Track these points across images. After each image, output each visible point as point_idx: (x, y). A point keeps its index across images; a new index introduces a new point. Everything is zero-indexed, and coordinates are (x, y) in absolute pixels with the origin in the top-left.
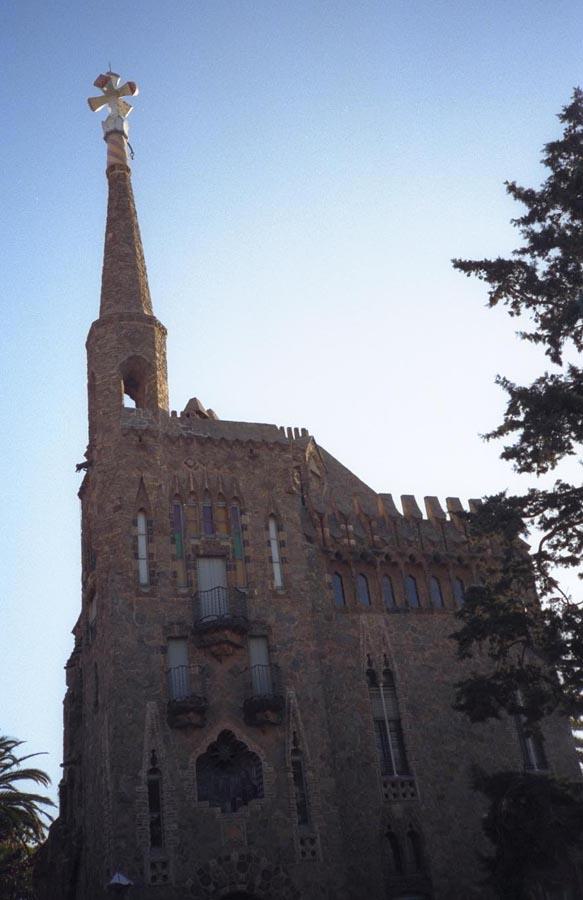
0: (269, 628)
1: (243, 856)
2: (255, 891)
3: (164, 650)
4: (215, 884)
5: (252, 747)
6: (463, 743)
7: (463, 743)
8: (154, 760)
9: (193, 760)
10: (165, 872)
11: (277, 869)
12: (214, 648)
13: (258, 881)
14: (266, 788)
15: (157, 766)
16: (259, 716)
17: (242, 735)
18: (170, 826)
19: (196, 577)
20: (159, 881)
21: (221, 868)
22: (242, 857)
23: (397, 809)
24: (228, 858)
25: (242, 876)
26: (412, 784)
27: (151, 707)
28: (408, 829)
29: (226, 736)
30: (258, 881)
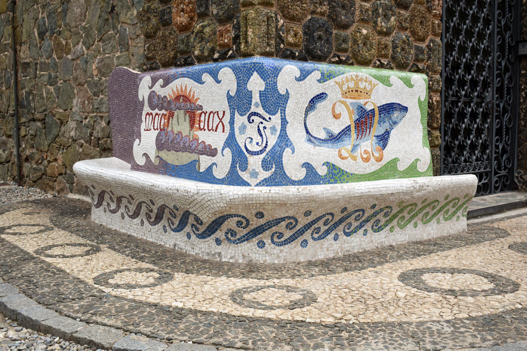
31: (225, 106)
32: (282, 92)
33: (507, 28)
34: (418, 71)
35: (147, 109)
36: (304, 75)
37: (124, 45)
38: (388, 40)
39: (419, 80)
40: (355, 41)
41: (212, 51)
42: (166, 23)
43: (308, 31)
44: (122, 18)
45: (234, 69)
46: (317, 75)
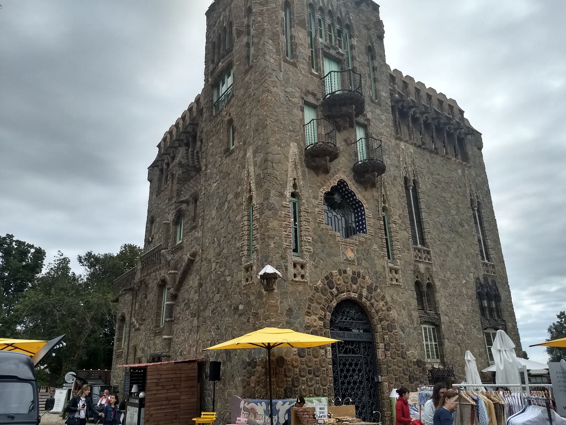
0: (368, 120)
1: (355, 272)
2: (364, 300)
3: (303, 111)
4: (337, 289)
5: (359, 197)
6: (453, 235)
7: (453, 235)
8: (295, 186)
9: (321, 194)
10: (303, 272)
11: (376, 286)
12: (338, 120)
13: (365, 293)
14: (368, 228)
15: (297, 191)
16: (367, 176)
17: (352, 186)
18: (307, 237)
19: (323, 67)
20: (298, 279)
21: (341, 278)
22: (354, 273)
23: (422, 267)
24: (345, 272)
25: (354, 286)
26: (428, 252)
27: (293, 150)
28: (428, 281)
29: (342, 183)
30: (365, 293)
31: (263, 413)
32: (278, 409)
33: (370, 371)
34: (324, 396)
35: (242, 411)
36: (284, 403)
37: (236, 388)
38: (312, 388)
39: (324, 400)
40: (300, 391)
41: (260, 396)
42: (249, 385)
43: (285, 390)
44: (236, 379)
45: (265, 402)
46: (288, 403)
